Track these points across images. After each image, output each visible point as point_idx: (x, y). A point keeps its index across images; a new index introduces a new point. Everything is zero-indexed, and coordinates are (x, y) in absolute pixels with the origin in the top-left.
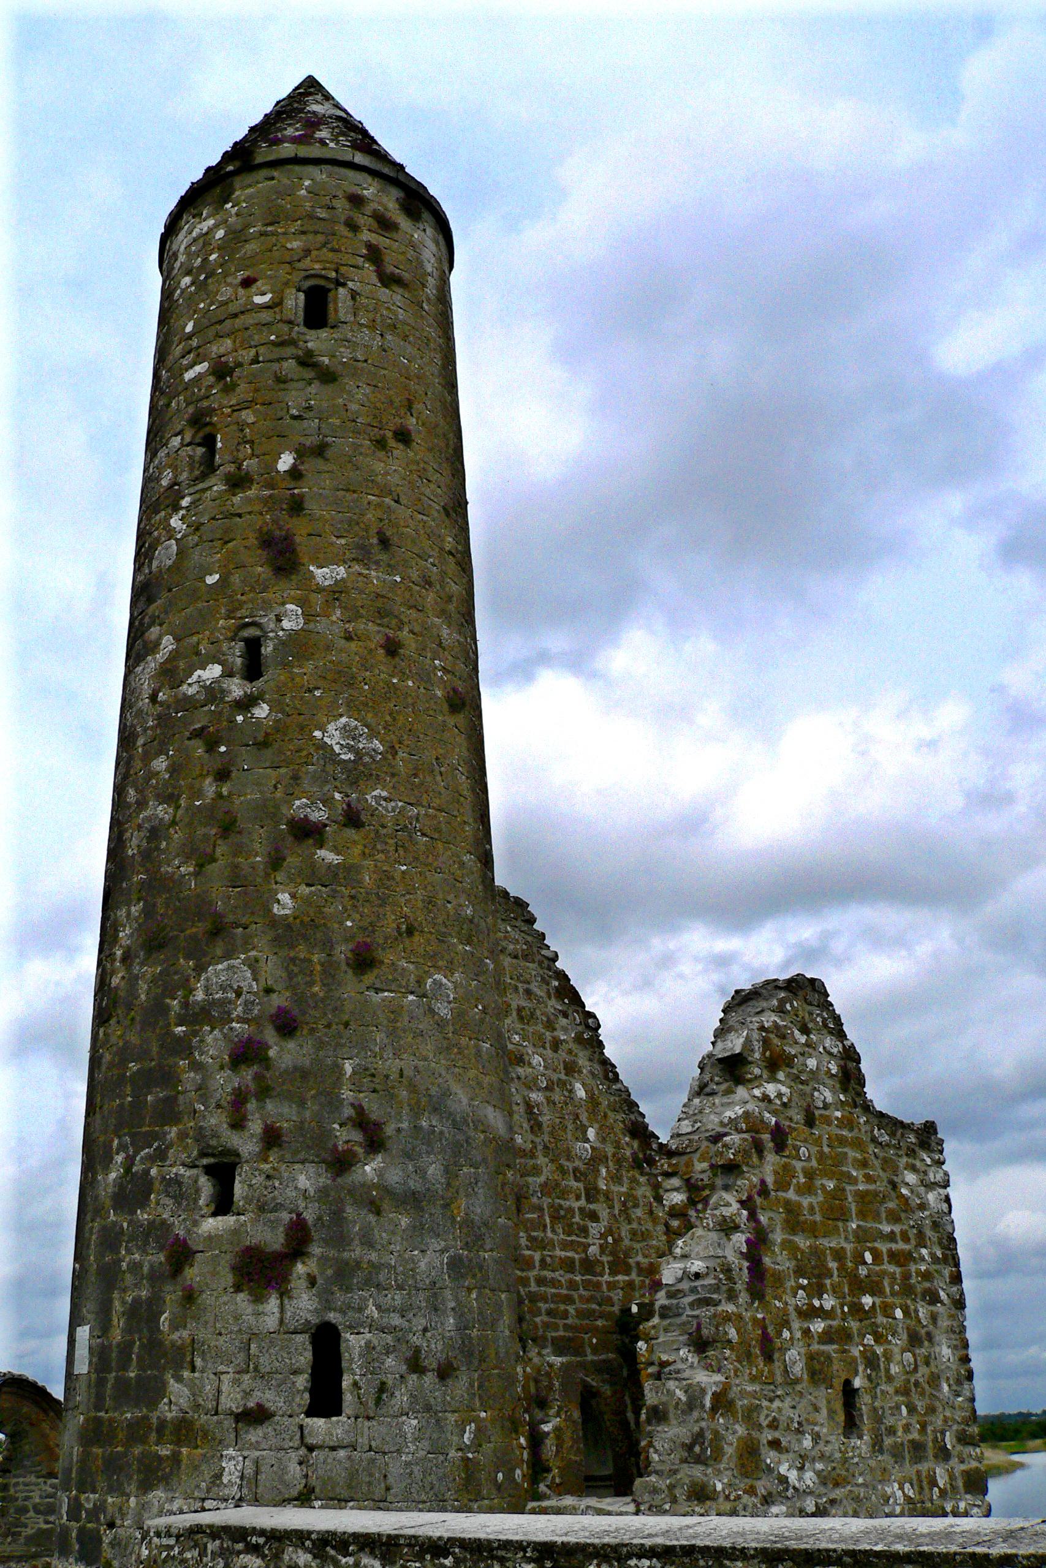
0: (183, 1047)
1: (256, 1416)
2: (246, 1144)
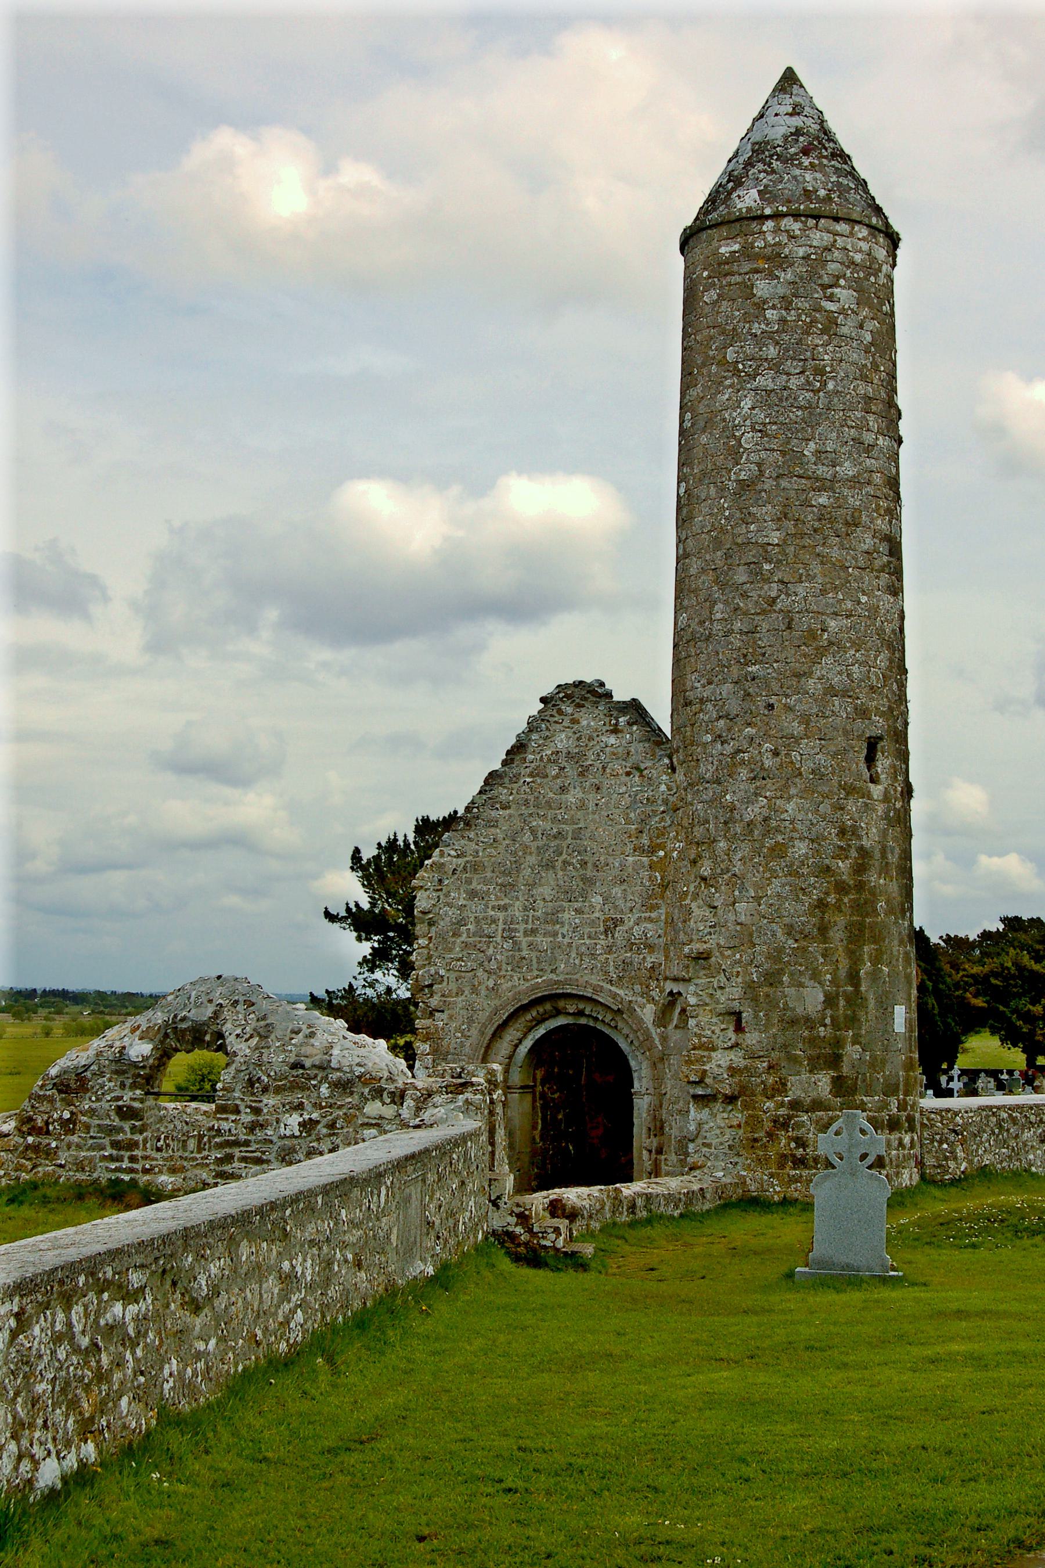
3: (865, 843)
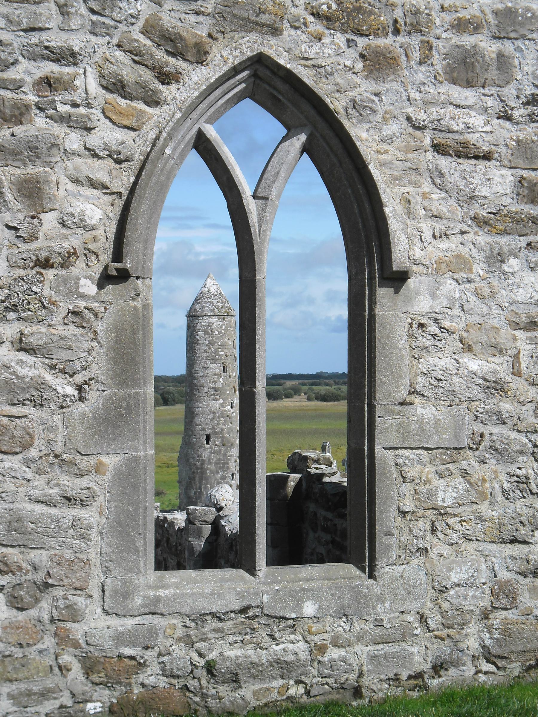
0: (229, 460)
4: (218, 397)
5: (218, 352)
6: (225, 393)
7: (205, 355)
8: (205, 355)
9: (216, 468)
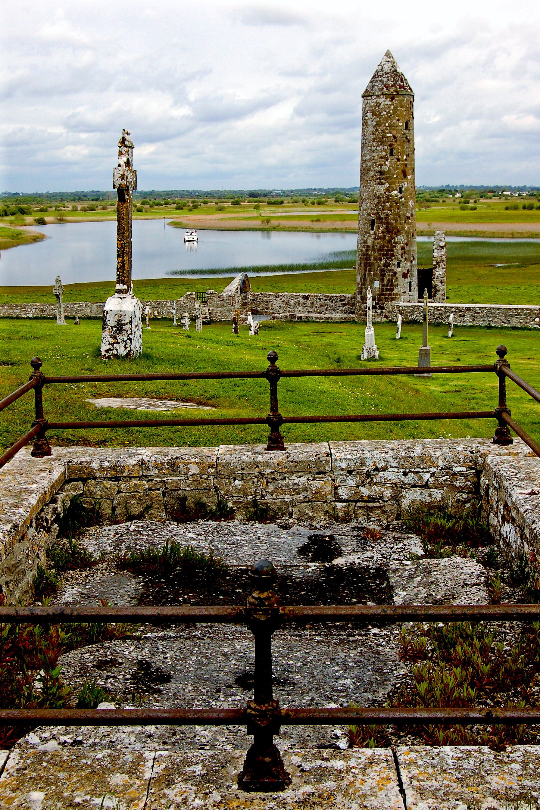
0: (394, 247)
1: (405, 292)
2: (403, 260)
3: (368, 244)
4: (384, 181)
5: (386, 133)
6: (392, 178)
7: (372, 136)
8: (372, 136)
9: (380, 255)
